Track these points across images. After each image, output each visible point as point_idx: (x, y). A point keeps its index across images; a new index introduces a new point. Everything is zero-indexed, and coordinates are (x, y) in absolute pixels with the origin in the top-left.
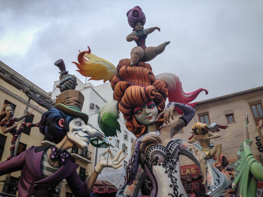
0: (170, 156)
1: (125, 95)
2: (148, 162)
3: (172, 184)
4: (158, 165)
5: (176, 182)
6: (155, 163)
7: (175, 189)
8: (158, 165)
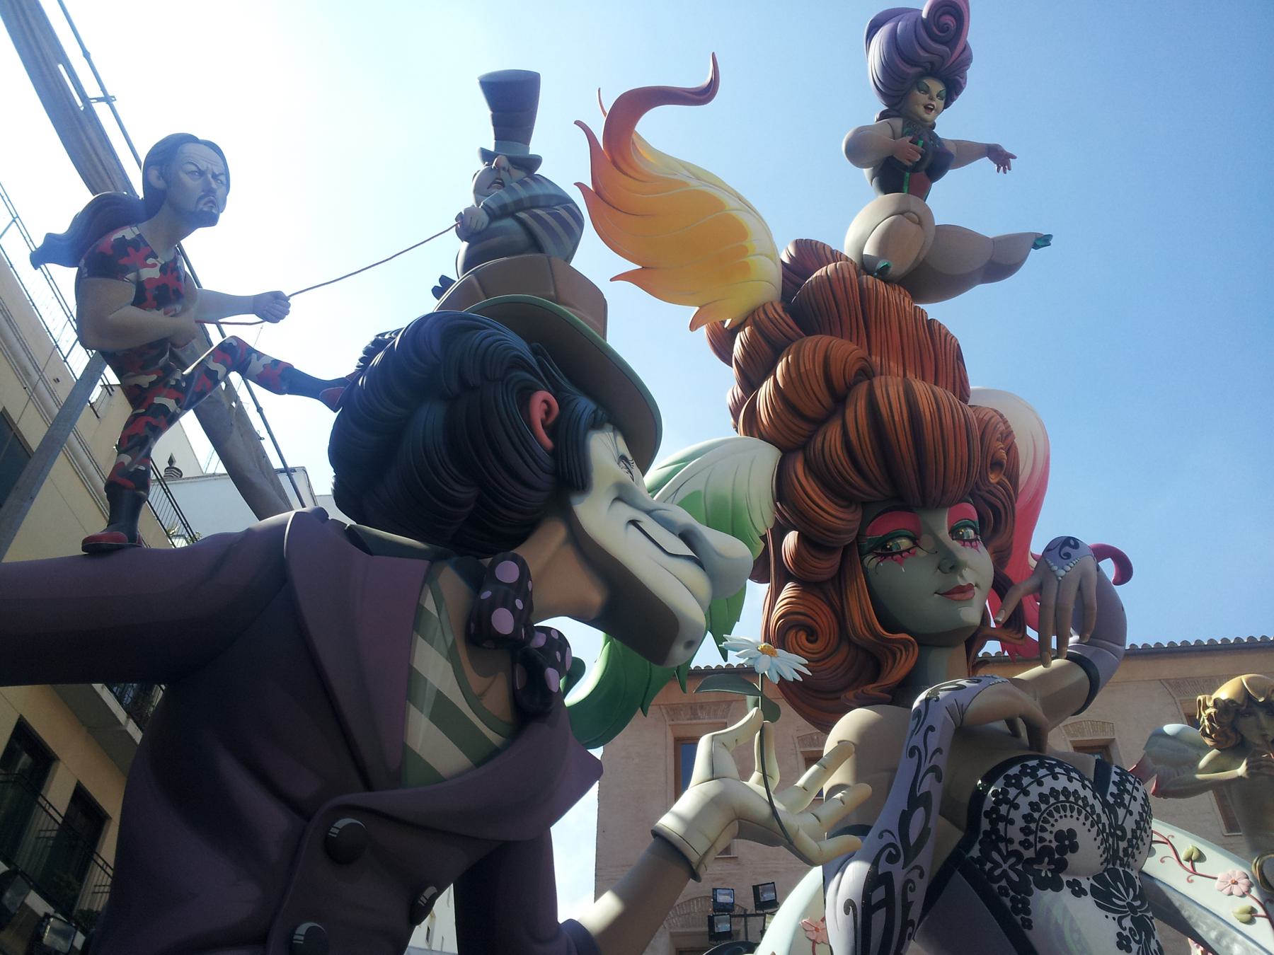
0: (1123, 845)
1: (857, 410)
2: (988, 866)
4: (1066, 892)
6: (1045, 871)
8: (1066, 891)
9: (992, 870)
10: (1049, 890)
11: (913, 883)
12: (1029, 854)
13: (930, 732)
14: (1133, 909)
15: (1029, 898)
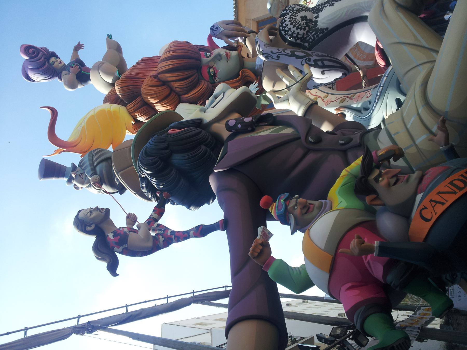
1: (169, 77)
2: (310, 40)
8: (317, 19)
10: (317, 23)
11: (317, 54)
12: (307, 28)
13: (273, 52)
15: (320, 29)
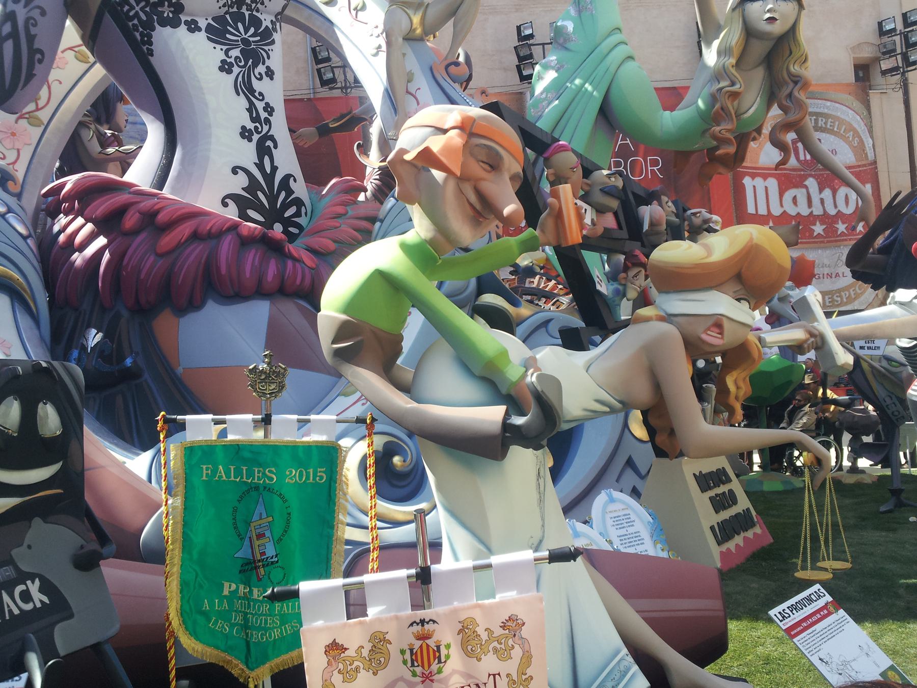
2: (126, 8)
3: (250, 125)
4: (183, 28)
5: (267, 121)
6: (167, 12)
7: (263, 151)
8: (183, 28)
9: (129, 11)
10: (169, 27)
14: (245, 42)
